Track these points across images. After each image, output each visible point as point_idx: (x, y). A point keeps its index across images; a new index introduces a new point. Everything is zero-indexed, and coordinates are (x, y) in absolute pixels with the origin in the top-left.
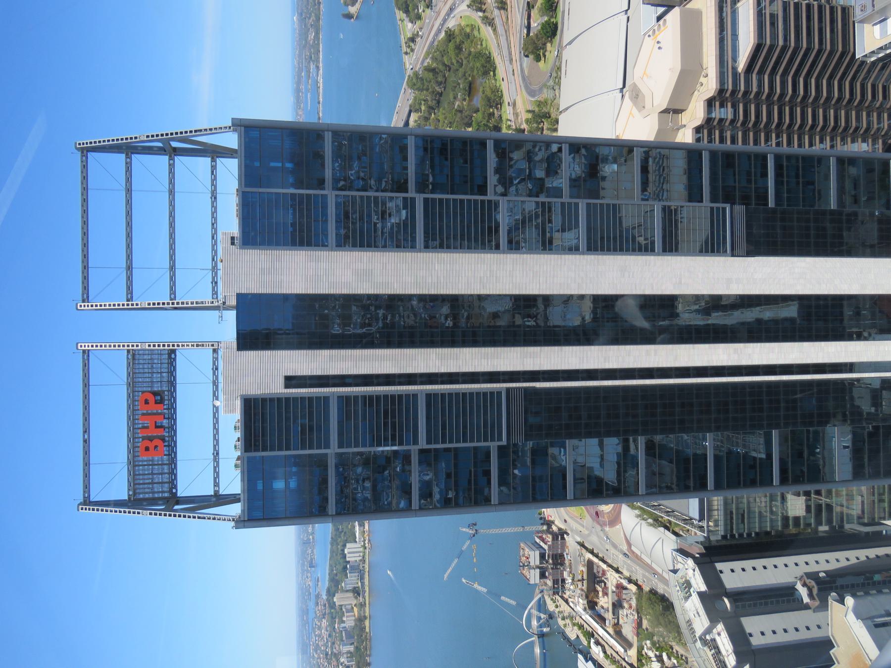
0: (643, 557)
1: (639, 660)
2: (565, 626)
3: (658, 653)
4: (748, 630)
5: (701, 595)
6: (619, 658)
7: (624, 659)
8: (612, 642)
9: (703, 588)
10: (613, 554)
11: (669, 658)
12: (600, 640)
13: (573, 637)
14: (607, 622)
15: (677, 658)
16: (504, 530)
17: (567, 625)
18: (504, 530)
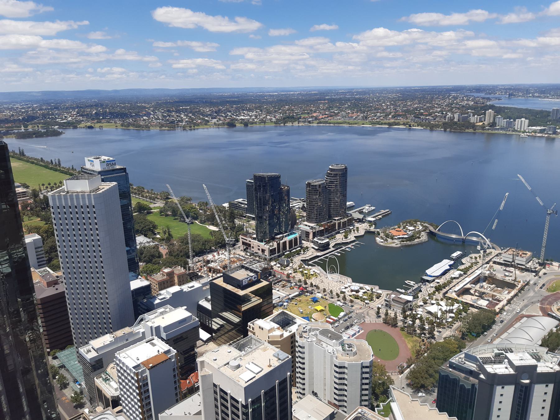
1: (450, 298)
2: (471, 258)
3: (454, 311)
6: (451, 286)
7: (450, 289)
10: (520, 303)
11: (450, 317)
12: (462, 278)
13: (463, 261)
15: (452, 322)
16: (546, 233)
17: (471, 259)
18: (546, 233)
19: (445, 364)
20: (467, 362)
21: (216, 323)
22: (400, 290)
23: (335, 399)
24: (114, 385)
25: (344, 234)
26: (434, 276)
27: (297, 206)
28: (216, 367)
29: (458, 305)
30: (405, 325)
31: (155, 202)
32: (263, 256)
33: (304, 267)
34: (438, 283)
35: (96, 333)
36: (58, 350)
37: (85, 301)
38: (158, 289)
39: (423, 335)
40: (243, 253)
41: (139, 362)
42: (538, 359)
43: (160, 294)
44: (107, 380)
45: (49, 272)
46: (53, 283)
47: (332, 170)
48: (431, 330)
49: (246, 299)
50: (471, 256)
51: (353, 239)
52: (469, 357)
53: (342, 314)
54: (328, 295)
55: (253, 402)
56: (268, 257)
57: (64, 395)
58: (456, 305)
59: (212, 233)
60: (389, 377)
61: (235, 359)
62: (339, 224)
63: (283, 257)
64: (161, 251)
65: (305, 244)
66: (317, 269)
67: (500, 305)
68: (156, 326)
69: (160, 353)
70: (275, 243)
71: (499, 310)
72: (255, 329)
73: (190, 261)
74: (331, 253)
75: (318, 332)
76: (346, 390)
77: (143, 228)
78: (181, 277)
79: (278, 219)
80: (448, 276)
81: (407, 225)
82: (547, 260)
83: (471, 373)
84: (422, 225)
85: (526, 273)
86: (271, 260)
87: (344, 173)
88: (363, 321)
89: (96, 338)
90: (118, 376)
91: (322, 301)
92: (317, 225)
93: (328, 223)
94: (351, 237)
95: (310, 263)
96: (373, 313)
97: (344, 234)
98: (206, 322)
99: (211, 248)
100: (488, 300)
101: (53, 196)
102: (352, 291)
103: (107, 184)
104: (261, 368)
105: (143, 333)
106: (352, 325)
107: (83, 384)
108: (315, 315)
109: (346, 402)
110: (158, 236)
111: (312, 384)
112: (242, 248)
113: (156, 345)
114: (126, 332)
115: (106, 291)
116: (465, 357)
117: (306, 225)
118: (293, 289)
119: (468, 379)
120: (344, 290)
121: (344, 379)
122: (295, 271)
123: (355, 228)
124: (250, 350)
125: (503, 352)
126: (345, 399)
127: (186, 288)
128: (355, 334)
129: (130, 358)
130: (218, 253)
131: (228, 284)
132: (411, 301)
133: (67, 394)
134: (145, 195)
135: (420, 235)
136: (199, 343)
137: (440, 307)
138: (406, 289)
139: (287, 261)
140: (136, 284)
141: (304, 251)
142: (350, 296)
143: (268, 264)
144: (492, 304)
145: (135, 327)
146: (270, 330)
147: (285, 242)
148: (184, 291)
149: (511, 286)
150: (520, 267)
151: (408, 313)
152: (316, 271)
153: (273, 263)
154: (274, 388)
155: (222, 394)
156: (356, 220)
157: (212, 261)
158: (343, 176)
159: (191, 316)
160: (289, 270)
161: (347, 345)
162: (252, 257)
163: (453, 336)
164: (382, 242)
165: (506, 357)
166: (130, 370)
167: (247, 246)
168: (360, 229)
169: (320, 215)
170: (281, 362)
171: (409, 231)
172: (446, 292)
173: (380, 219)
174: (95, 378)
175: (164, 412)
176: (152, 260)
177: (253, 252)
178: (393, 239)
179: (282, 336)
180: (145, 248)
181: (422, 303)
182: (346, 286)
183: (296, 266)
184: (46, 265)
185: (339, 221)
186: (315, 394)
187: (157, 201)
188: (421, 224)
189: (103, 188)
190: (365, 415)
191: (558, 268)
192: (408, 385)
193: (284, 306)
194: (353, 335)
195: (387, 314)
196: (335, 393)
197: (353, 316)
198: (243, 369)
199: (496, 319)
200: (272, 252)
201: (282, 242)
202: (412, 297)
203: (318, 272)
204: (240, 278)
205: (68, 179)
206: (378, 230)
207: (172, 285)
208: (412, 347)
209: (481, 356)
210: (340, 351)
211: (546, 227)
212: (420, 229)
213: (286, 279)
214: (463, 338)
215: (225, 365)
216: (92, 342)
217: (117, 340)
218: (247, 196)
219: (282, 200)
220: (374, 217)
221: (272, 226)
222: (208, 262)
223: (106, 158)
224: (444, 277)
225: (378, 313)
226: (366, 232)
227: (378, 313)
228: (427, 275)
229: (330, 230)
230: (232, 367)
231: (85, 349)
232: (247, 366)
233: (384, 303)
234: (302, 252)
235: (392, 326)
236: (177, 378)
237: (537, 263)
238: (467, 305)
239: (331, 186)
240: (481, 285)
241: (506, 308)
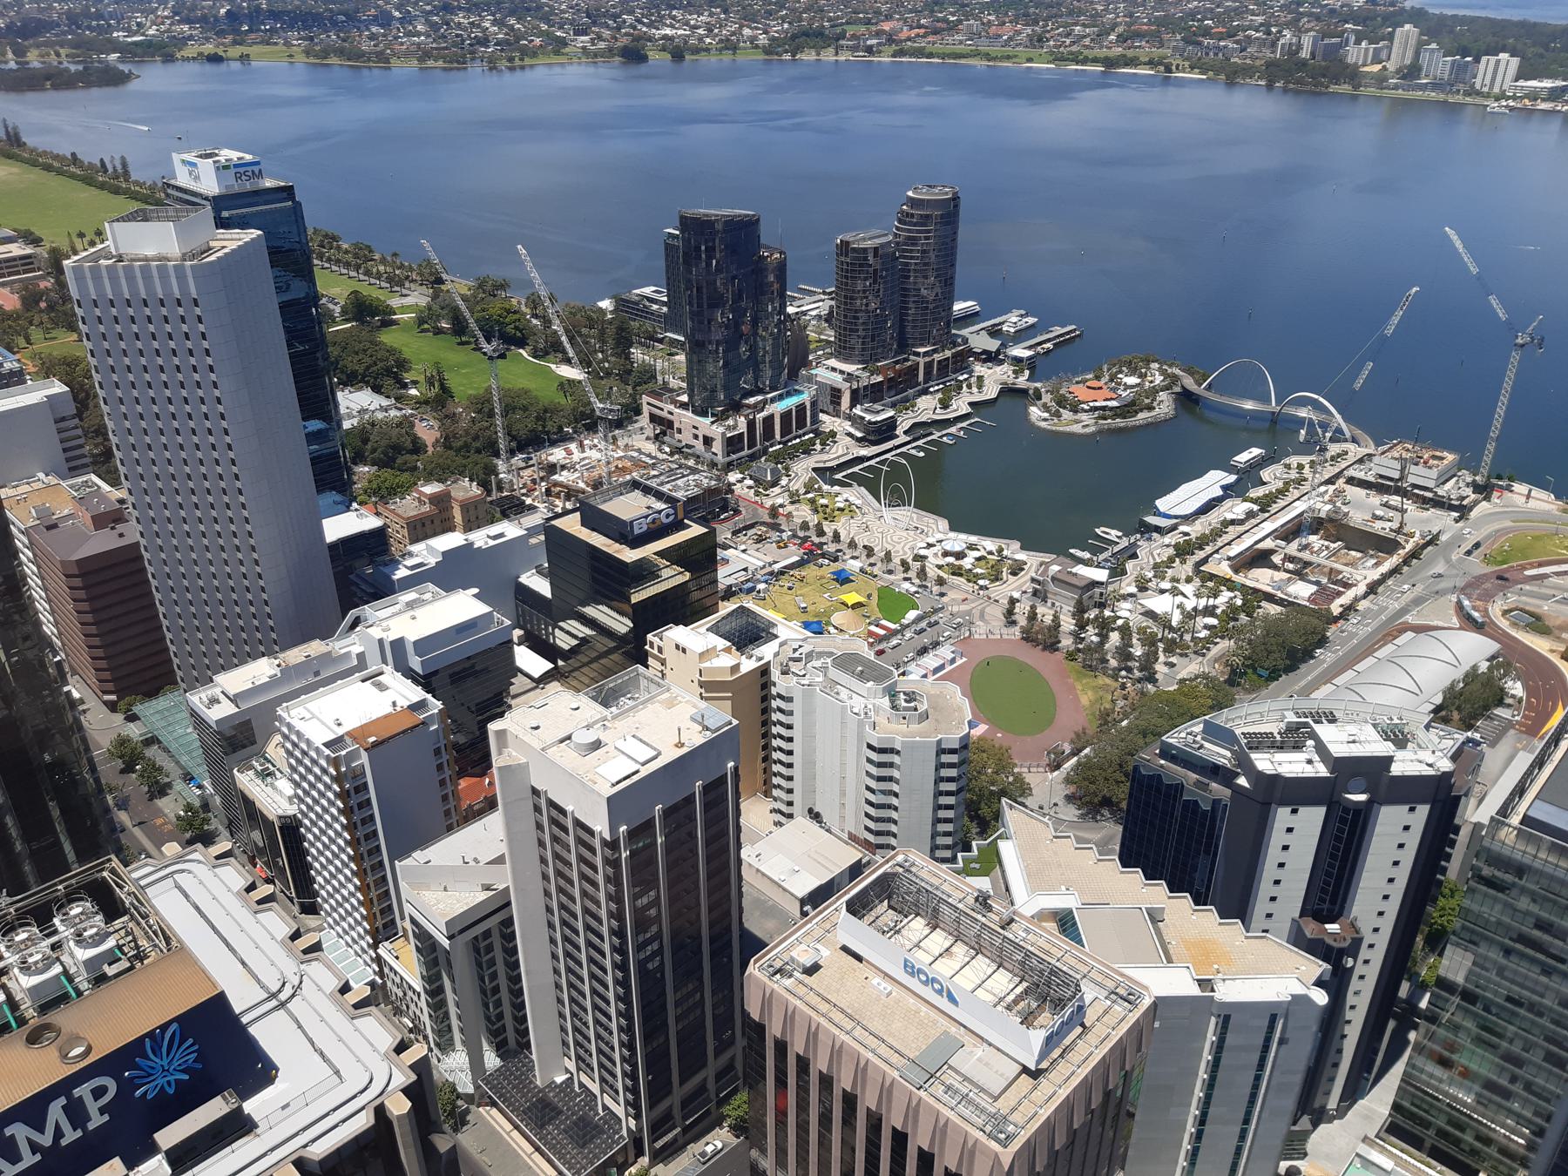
0: (1389, 648)
1: (1212, 577)
2: (1288, 467)
3: (1219, 611)
4: (1302, 810)
5: (1389, 760)
6: (1220, 544)
7: (1217, 552)
8: (1247, 542)
9: (1396, 769)
11: (1206, 627)
12: (1254, 521)
13: (1266, 474)
14: (1283, 543)
15: (1208, 640)
16: (1504, 399)
18: (1504, 399)
19: (1149, 749)
20: (1207, 745)
21: (568, 633)
22: (1079, 553)
23: (867, 828)
25: (940, 395)
26: (1176, 517)
27: (814, 313)
28: (537, 745)
29: (1232, 595)
30: (1081, 646)
31: (404, 292)
32: (708, 456)
33: (820, 488)
34: (1186, 534)
35: (234, 655)
36: (139, 698)
37: (197, 569)
39: (1123, 673)
40: (651, 448)
41: (341, 731)
42: (1400, 739)
43: (411, 554)
44: (268, 775)
45: (99, 487)
46: (109, 519)
47: (913, 203)
48: (1147, 661)
49: (643, 572)
50: (1287, 461)
51: (965, 409)
52: (1217, 733)
53: (912, 615)
54: (879, 564)
55: (632, 835)
56: (720, 459)
57: (159, 813)
58: (1225, 595)
59: (567, 386)
60: (1019, 779)
61: (588, 727)
62: (928, 366)
63: (763, 459)
64: (420, 435)
65: (828, 422)
66: (855, 495)
67: (1345, 599)
68: (391, 639)
69: (398, 709)
70: (743, 419)
71: (1341, 609)
72: (665, 650)
73: (501, 465)
74: (899, 451)
75: (829, 660)
76: (896, 809)
77: (368, 368)
79: (753, 349)
80: (1214, 517)
81: (1121, 372)
82: (1500, 478)
83: (1214, 771)
84: (1163, 372)
85: (1433, 512)
86: (729, 467)
87: (949, 213)
88: (967, 634)
90: (291, 766)
91: (860, 580)
92: (864, 369)
93: (897, 362)
94: (960, 405)
95: (839, 476)
96: (996, 613)
97: (940, 395)
98: (540, 630)
99: (560, 428)
100: (1317, 583)
101: (77, 270)
102: (946, 554)
103: (234, 236)
104: (655, 749)
105: (361, 656)
106: (936, 644)
107: (207, 783)
108: (837, 618)
109: (895, 836)
110: (413, 392)
111: (810, 790)
112: (649, 432)
114: (313, 654)
115: (252, 541)
116: (1204, 731)
117: (834, 369)
118: (786, 547)
119: (1205, 787)
120: (923, 552)
121: (891, 779)
122: (795, 499)
123: (973, 380)
124: (631, 703)
125: (1309, 720)
126: (894, 828)
127: (481, 538)
128: (942, 667)
130: (581, 446)
131: (593, 530)
132: (1102, 583)
133: (167, 811)
134: (375, 270)
135: (1153, 400)
136: (519, 683)
137: (1179, 599)
138: (1096, 551)
139: (774, 472)
140: (339, 526)
141: (823, 444)
142: (940, 567)
143: (718, 479)
144: (1325, 595)
145: (340, 638)
146: (703, 656)
147: (770, 418)
149: (1385, 545)
150: (1418, 495)
151: (1092, 614)
152: (851, 499)
153: (733, 477)
154: (690, 799)
155: (554, 813)
156: (977, 356)
157: (563, 467)
158: (948, 223)
160: (776, 497)
161: (905, 693)
162: (676, 456)
163: (1205, 676)
164: (1045, 420)
165: (1313, 735)
166: (317, 750)
167: (664, 426)
168: (986, 382)
169: (873, 340)
170: (709, 735)
171: (1125, 390)
172: (1205, 561)
173: (1049, 351)
174: (235, 771)
176: (394, 460)
177: (680, 445)
178: (1076, 411)
179: (735, 668)
180: (373, 425)
181: (1133, 589)
182: (931, 540)
183: (797, 485)
184: (90, 468)
185: (928, 359)
186: (815, 816)
187: (409, 289)
188: (1160, 369)
189: (223, 247)
190: (913, 869)
191: (1524, 499)
192: (1070, 799)
193: (759, 592)
194: (936, 670)
195: (1032, 616)
196: (867, 815)
197: (941, 621)
199: (1328, 634)
200: (733, 444)
201: (760, 416)
202: (1106, 572)
203: (858, 502)
204: (625, 516)
205: (118, 220)
206: (1038, 385)
207: (447, 527)
208: (1092, 704)
209: (1246, 730)
210: (884, 710)
211: (1508, 385)
212: (1157, 382)
213: (767, 519)
214: (1231, 682)
215: (562, 741)
216: (220, 678)
217: (288, 673)
218: (668, 278)
219: (763, 294)
220: (1030, 348)
221: (733, 369)
222: (552, 468)
223: (234, 155)
224: (1203, 519)
225: (1010, 612)
226: (1001, 392)
227: (1010, 612)
228: (1158, 513)
229: (900, 383)
230: (578, 746)
231: (203, 696)
232: (620, 744)
233: (1029, 587)
234: (818, 447)
235: (1044, 649)
236: (448, 773)
237: (1468, 485)
238: (1255, 596)
239: (911, 251)
240: (1304, 541)
241: (1363, 605)
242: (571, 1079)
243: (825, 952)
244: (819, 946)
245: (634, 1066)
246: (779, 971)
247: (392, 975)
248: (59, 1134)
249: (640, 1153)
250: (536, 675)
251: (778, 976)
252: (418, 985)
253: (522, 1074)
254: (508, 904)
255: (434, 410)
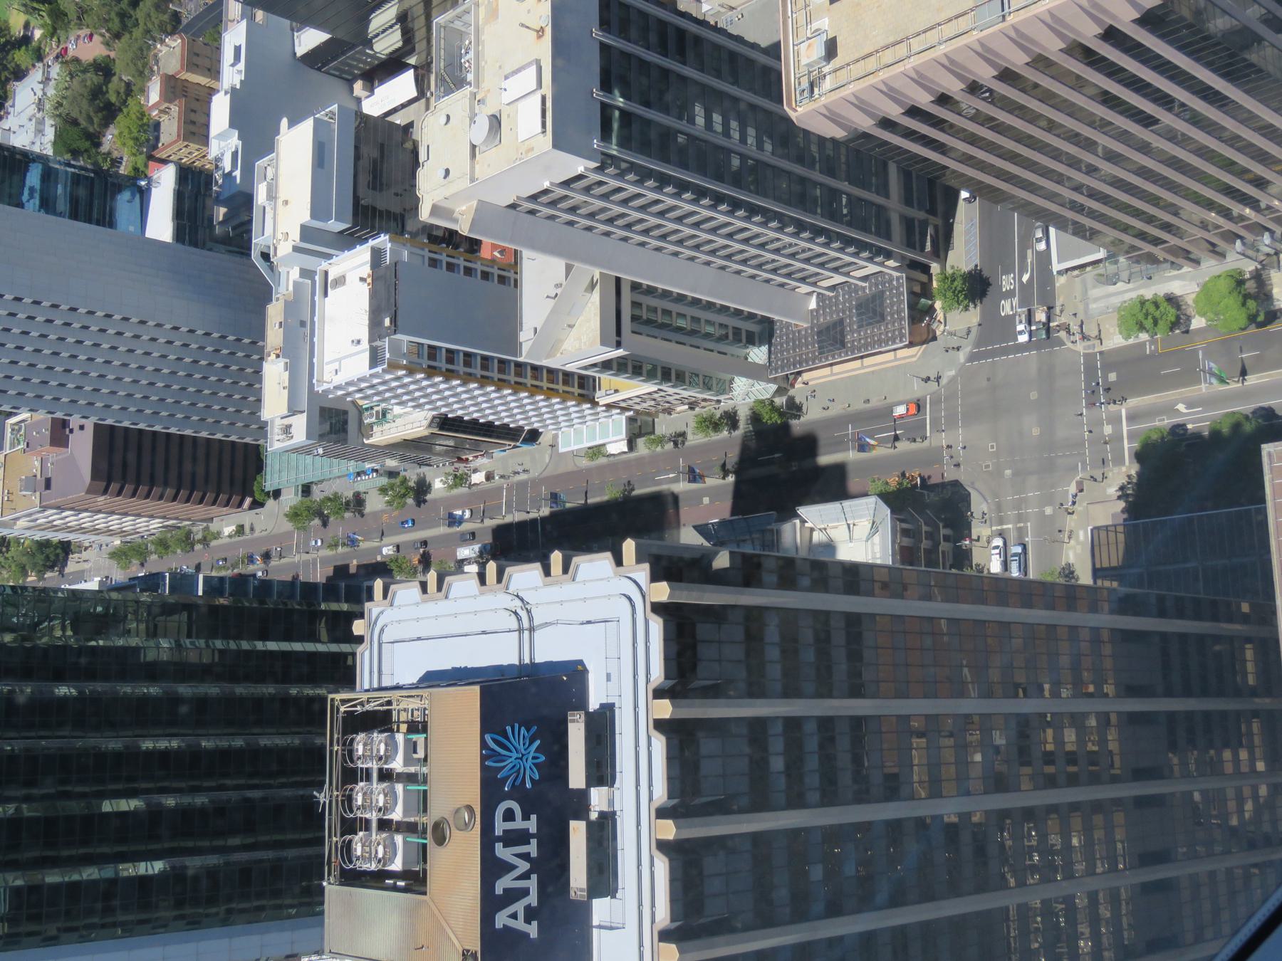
24: (397, 410)
28: (466, 183)
36: (258, 478)
38: (205, 149)
41: (365, 345)
43: (218, 159)
44: (384, 415)
46: (60, 434)
57: (375, 514)
61: (472, 120)
68: (297, 237)
69: (369, 280)
78: (195, 59)
89: (259, 400)
98: (365, 62)
105: (306, 273)
113: (344, 277)
124: (471, 55)
127: (232, 75)
129: (345, 357)
148: (238, 87)
154: (604, 47)
155: (544, 199)
159: (317, 121)
175: (521, 344)
180: (60, 105)
198: (509, 116)
215: (473, 155)
216: (266, 414)
232: (506, 97)
236: (461, 262)
242: (819, 294)
243: (823, 23)
244: (815, 25)
245: (840, 237)
246: (812, 85)
247: (630, 402)
248: (525, 857)
249: (926, 269)
250: (414, 94)
251: (816, 90)
252: (649, 387)
253: (787, 335)
254: (618, 280)
255: (66, 27)
